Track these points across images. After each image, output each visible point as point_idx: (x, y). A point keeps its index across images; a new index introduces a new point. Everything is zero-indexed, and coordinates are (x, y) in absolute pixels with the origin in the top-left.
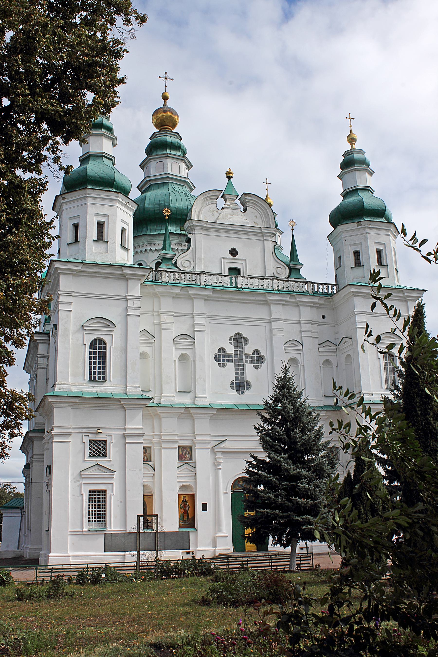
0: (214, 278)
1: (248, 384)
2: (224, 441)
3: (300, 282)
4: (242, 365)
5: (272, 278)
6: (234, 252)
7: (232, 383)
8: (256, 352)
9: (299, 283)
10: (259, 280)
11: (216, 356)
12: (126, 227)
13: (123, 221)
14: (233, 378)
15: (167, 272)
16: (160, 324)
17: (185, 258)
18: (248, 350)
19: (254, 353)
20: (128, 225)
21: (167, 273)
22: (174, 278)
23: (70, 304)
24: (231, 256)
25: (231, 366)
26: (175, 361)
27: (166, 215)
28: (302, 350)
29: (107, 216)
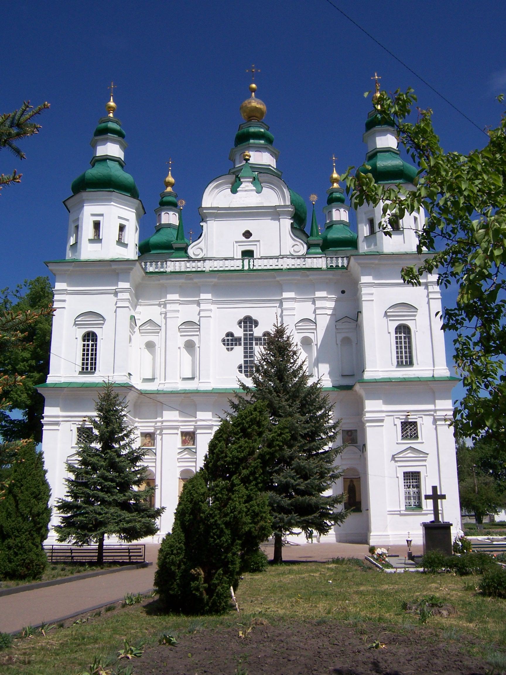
0: (221, 263)
3: (314, 258)
4: (251, 348)
6: (247, 234)
10: (268, 260)
11: (224, 340)
12: (123, 222)
13: (120, 218)
16: (166, 314)
19: (264, 335)
22: (180, 267)
23: (64, 301)
24: (244, 239)
25: (239, 350)
26: (179, 348)
28: (316, 329)
29: (102, 215)
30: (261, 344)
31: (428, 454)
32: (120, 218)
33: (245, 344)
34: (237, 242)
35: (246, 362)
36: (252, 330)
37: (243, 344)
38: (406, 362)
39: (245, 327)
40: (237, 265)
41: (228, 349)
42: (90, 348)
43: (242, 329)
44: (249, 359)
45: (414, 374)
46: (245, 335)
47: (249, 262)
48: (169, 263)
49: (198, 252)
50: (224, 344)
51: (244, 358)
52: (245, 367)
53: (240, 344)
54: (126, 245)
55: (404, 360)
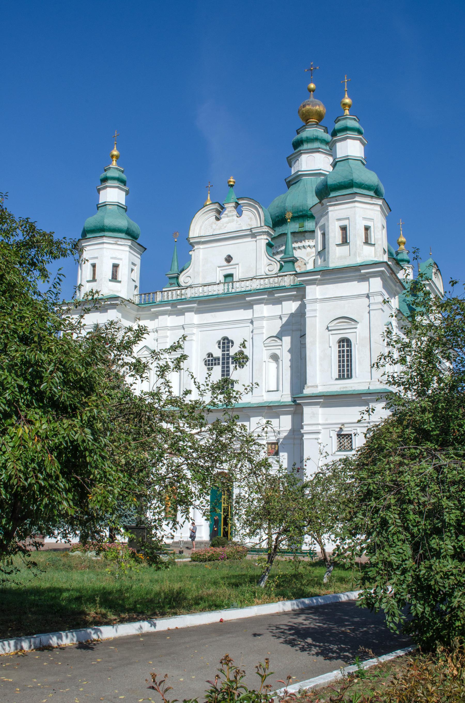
6: (229, 259)
11: (206, 362)
12: (116, 262)
17: (187, 275)
24: (225, 263)
29: (97, 258)
32: (112, 258)
33: (223, 363)
34: (219, 267)
36: (228, 350)
38: (348, 375)
39: (224, 347)
40: (219, 290)
45: (351, 387)
46: (223, 355)
47: (228, 286)
50: (206, 364)
53: (219, 364)
55: (346, 373)
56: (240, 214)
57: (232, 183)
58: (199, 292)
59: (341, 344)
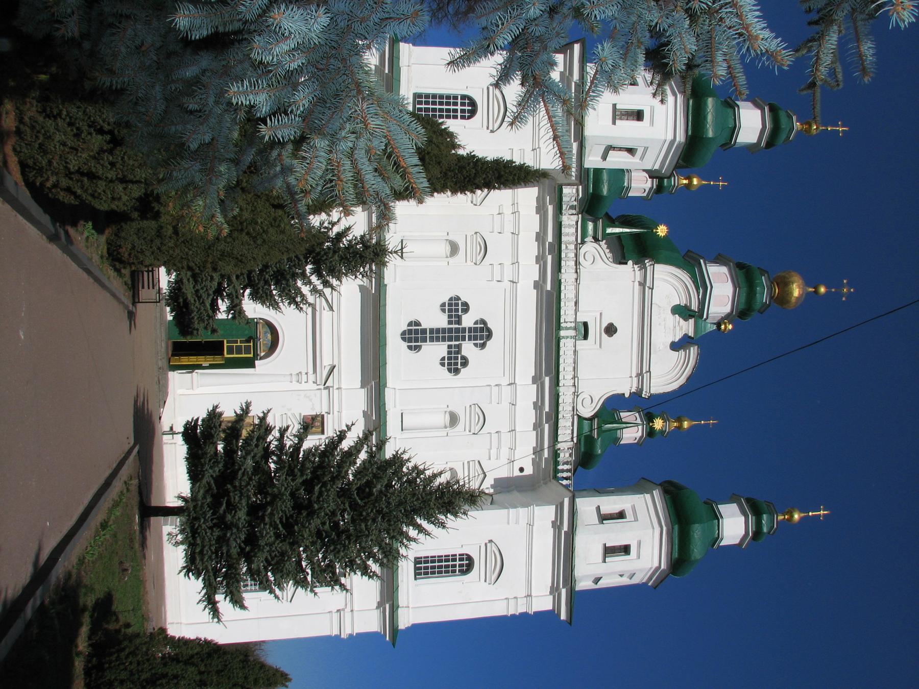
0: (572, 295)
1: (417, 348)
2: (332, 308)
3: (573, 430)
4: (444, 339)
5: (576, 384)
6: (611, 330)
7: (417, 324)
8: (465, 362)
9: (571, 428)
14: (426, 325)
15: (577, 222)
18: (468, 349)
19: (464, 358)
20: (642, 158)
21: (574, 223)
22: (568, 235)
24: (604, 325)
25: (441, 321)
27: (657, 229)
29: (652, 123)
30: (449, 353)
31: (291, 601)
33: (450, 330)
35: (424, 331)
36: (470, 339)
37: (451, 326)
38: (420, 568)
39: (476, 329)
40: (567, 314)
41: (443, 305)
42: (452, 107)
43: (472, 325)
44: (428, 335)
45: (403, 581)
48: (575, 218)
49: (589, 258)
50: (451, 299)
51: (430, 329)
52: (416, 331)
53: (450, 323)
54: (604, 157)
55: (423, 565)
56: (675, 346)
57: (723, 327)
58: (567, 292)
59: (465, 557)
